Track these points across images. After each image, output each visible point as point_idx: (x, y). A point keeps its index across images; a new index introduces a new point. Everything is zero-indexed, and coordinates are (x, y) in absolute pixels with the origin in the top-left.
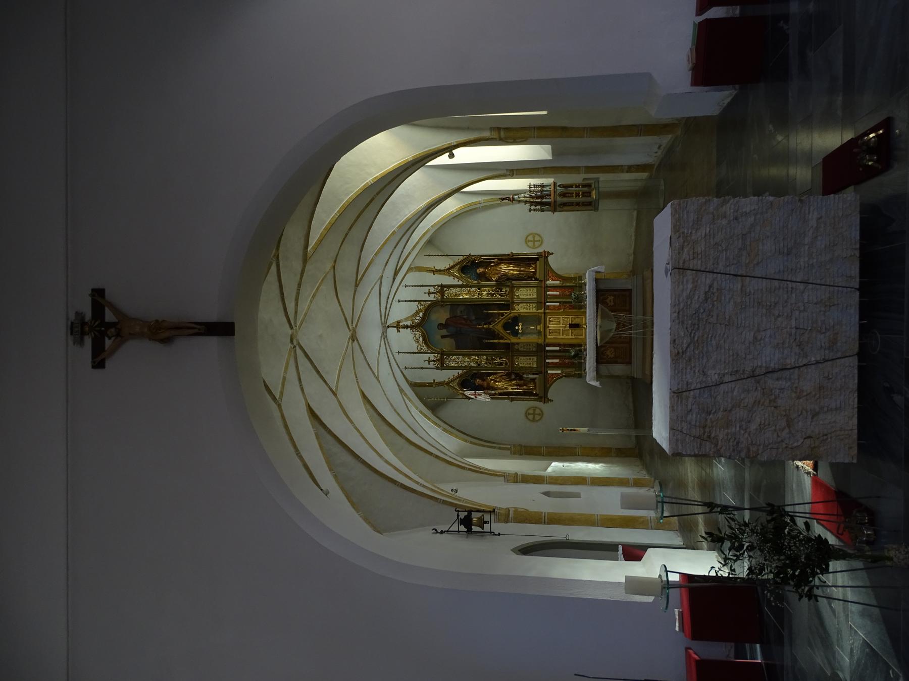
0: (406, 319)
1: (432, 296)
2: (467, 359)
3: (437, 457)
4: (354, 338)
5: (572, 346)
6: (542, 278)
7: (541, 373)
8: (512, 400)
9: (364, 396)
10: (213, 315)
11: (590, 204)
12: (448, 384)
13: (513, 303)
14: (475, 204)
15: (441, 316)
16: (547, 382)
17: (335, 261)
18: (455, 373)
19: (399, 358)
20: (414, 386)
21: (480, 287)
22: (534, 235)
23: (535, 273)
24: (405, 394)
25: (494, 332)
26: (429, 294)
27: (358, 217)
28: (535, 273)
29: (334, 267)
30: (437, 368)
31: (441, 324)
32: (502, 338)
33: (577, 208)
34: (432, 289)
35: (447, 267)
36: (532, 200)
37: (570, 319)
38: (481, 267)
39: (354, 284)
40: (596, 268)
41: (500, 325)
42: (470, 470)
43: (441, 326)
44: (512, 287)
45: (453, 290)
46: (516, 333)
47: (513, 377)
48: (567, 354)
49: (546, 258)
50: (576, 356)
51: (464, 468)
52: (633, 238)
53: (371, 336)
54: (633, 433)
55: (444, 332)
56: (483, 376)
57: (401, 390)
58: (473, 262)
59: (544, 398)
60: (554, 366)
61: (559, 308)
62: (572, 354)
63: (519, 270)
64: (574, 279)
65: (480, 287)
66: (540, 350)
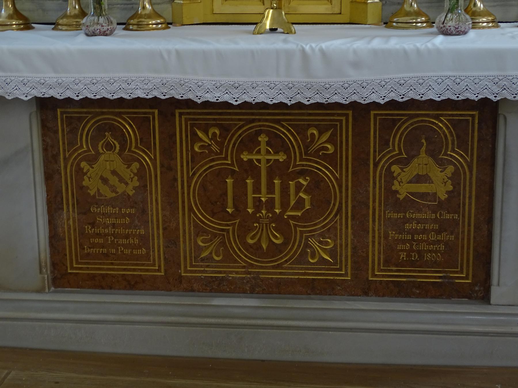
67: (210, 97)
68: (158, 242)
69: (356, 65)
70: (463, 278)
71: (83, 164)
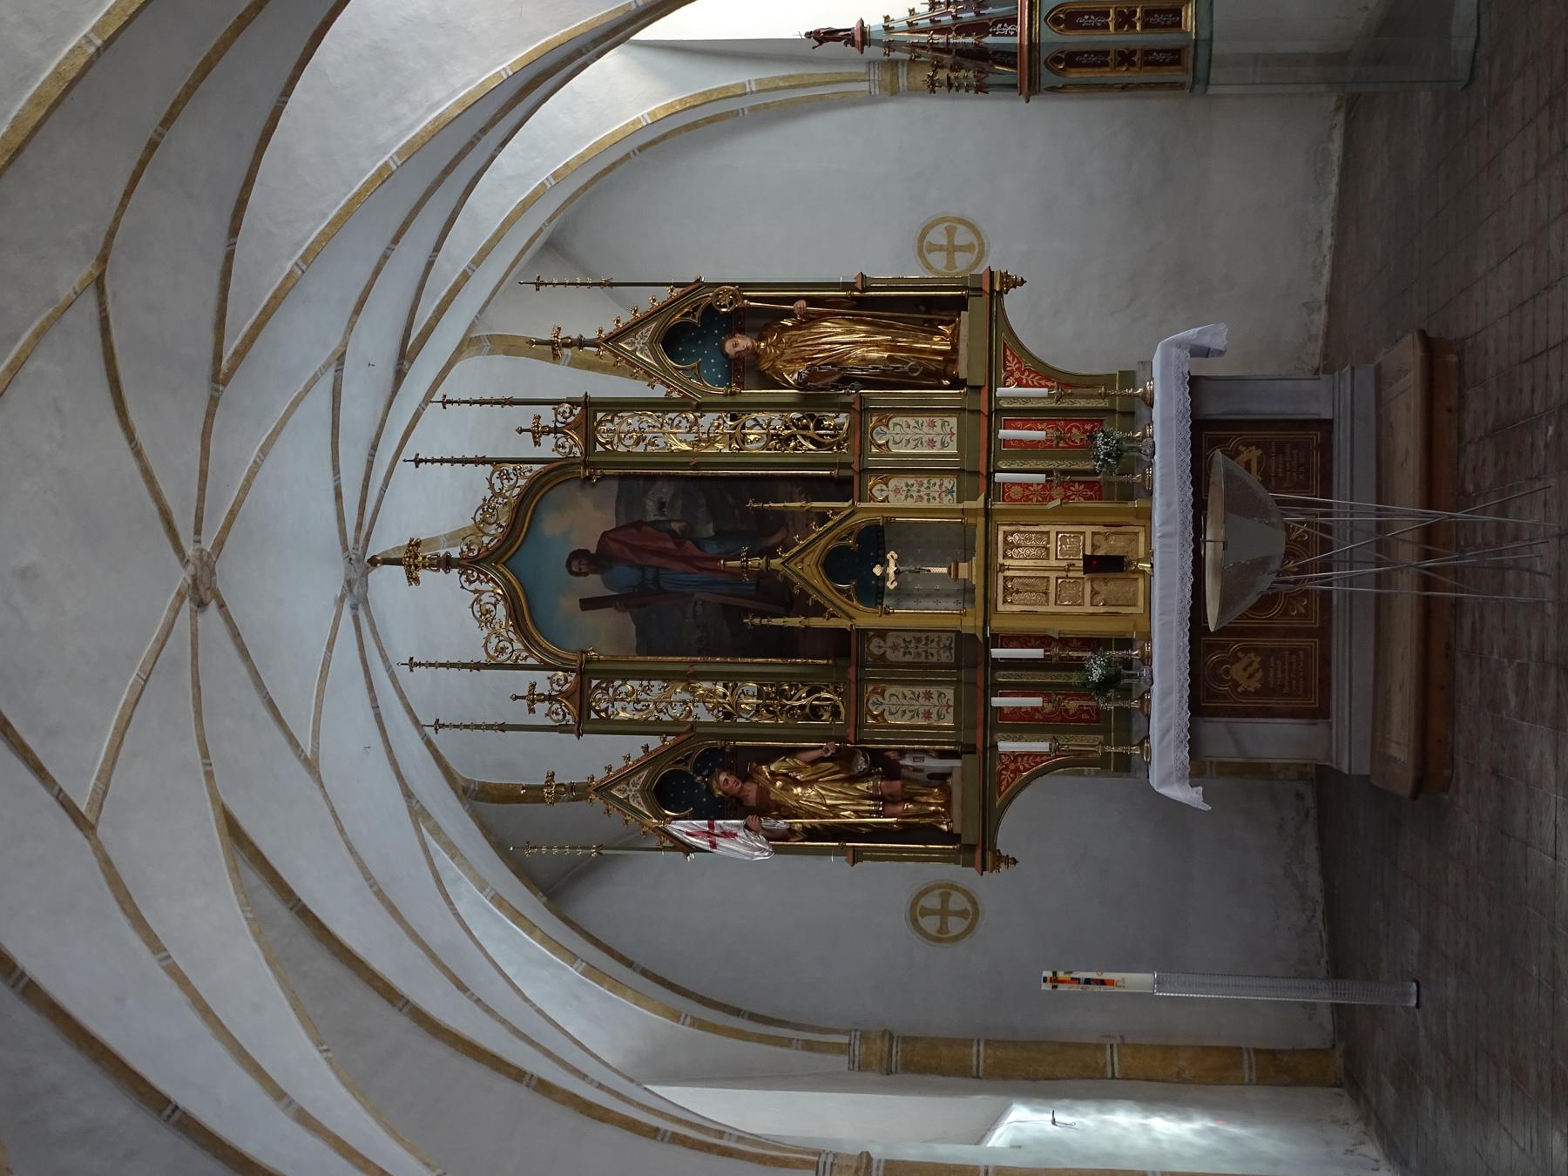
0: (452, 538)
1: (548, 441)
2: (679, 693)
3: (544, 1087)
4: (202, 592)
5: (1093, 643)
6: (979, 378)
7: (971, 750)
8: (857, 857)
9: (234, 832)
11: (1174, 57)
12: (603, 790)
13: (864, 471)
14: (726, 95)
15: (584, 520)
16: (994, 789)
17: (103, 259)
18: (633, 747)
19: (419, 683)
20: (477, 796)
21: (736, 411)
22: (952, 223)
23: (951, 357)
24: (436, 831)
25: (788, 583)
26: (537, 433)
27: (204, 70)
28: (951, 357)
29: (99, 283)
30: (562, 729)
31: (578, 555)
32: (819, 610)
33: (1124, 75)
34: (547, 416)
35: (609, 328)
36: (940, 39)
37: (1088, 538)
38: (742, 331)
39: (206, 369)
40: (1191, 333)
41: (811, 559)
42: (677, 1139)
43: (581, 561)
44: (862, 412)
45: (632, 421)
46: (873, 593)
47: (861, 764)
48: (1075, 678)
49: (996, 297)
50: (1109, 683)
51: (653, 1133)
52: (1328, 241)
53: (290, 594)
54: (1324, 997)
55: (593, 585)
56: (743, 761)
57: (419, 813)
58: (710, 311)
59: (981, 850)
60: (1023, 724)
61: (1045, 493)
62: (1096, 674)
63: (893, 347)
64: (1108, 380)
65: (736, 411)
66: (970, 661)
67: (1189, 595)
68: (1295, 642)
69: (1169, 505)
70: (1317, 437)
71: (1240, 690)
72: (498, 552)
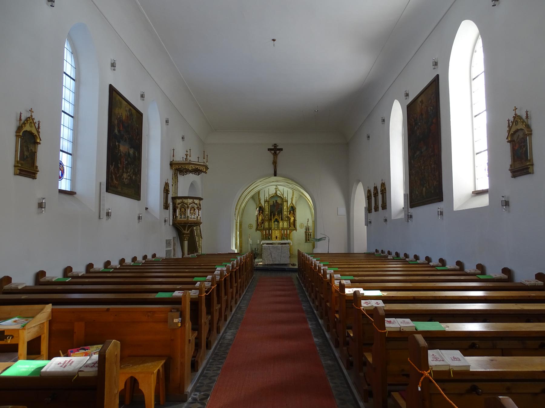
10: (278, 172)
15: (279, 201)
18: (263, 205)
20: (259, 192)
43: (276, 201)
46: (275, 222)
56: (262, 213)
59: (257, 229)
60: (266, 232)
66: (270, 229)
72: (276, 195)
